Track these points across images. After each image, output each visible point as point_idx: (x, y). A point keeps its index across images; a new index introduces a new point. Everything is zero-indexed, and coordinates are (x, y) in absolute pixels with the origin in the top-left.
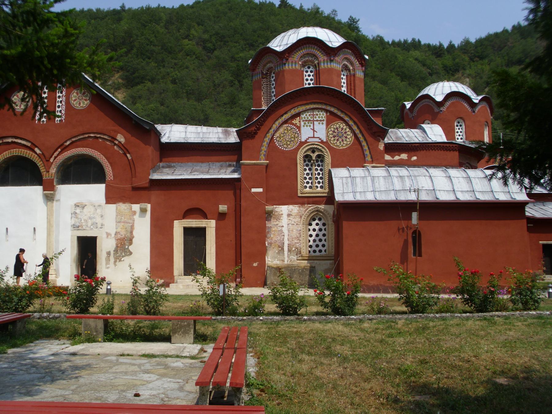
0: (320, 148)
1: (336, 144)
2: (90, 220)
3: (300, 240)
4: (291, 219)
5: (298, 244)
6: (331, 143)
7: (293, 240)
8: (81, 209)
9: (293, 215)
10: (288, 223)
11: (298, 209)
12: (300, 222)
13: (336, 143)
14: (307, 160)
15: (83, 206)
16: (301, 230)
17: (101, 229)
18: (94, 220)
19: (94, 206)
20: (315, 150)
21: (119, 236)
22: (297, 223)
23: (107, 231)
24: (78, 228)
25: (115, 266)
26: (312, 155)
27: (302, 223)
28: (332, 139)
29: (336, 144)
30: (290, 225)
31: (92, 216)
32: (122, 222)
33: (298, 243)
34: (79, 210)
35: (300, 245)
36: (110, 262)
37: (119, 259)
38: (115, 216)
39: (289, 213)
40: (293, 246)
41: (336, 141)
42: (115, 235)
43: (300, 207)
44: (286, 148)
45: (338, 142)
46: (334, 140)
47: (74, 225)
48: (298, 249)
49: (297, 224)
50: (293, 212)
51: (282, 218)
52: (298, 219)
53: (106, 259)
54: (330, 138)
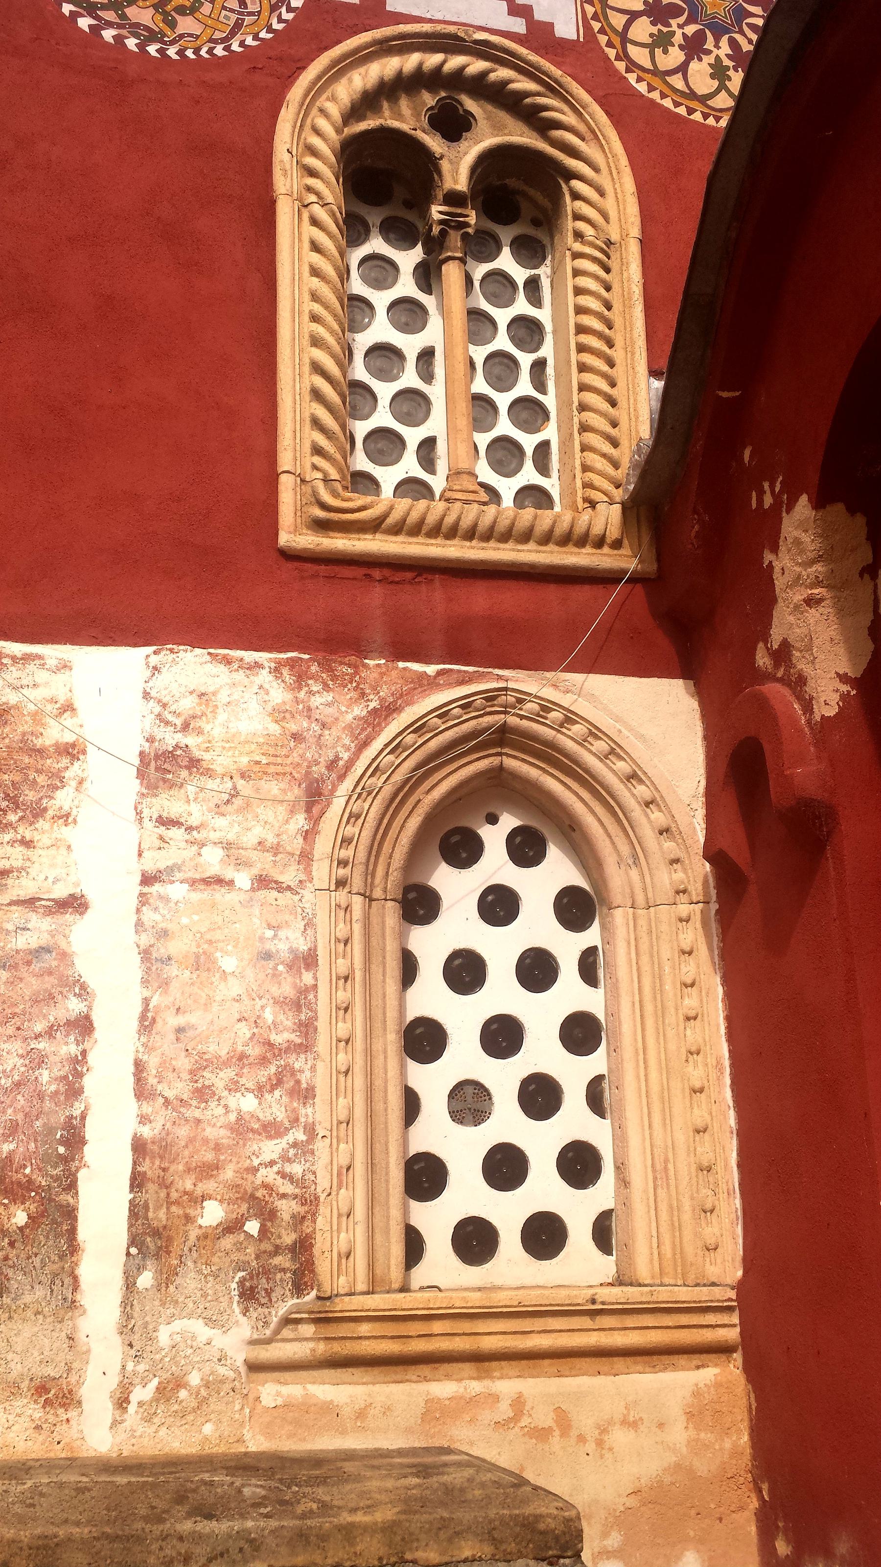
0: (524, 84)
1: (677, 82)
3: (307, 1095)
4: (196, 814)
5: (271, 1149)
6: (632, 66)
7: (203, 1094)
9: (221, 761)
10: (153, 861)
11: (278, 694)
12: (306, 858)
13: (683, 69)
14: (374, 217)
16: (309, 960)
20: (470, 104)
22: (263, 863)
26: (434, 143)
27: (322, 872)
28: (642, 29)
29: (677, 82)
30: (177, 891)
33: (272, 1130)
35: (303, 1149)
39: (170, 739)
40: (208, 1170)
41: (675, 56)
43: (301, 678)
44: (153, 36)
45: (700, 70)
46: (662, 41)
48: (268, 1215)
49: (263, 882)
50: (215, 728)
51: (63, 798)
52: (273, 814)
54: (618, 21)
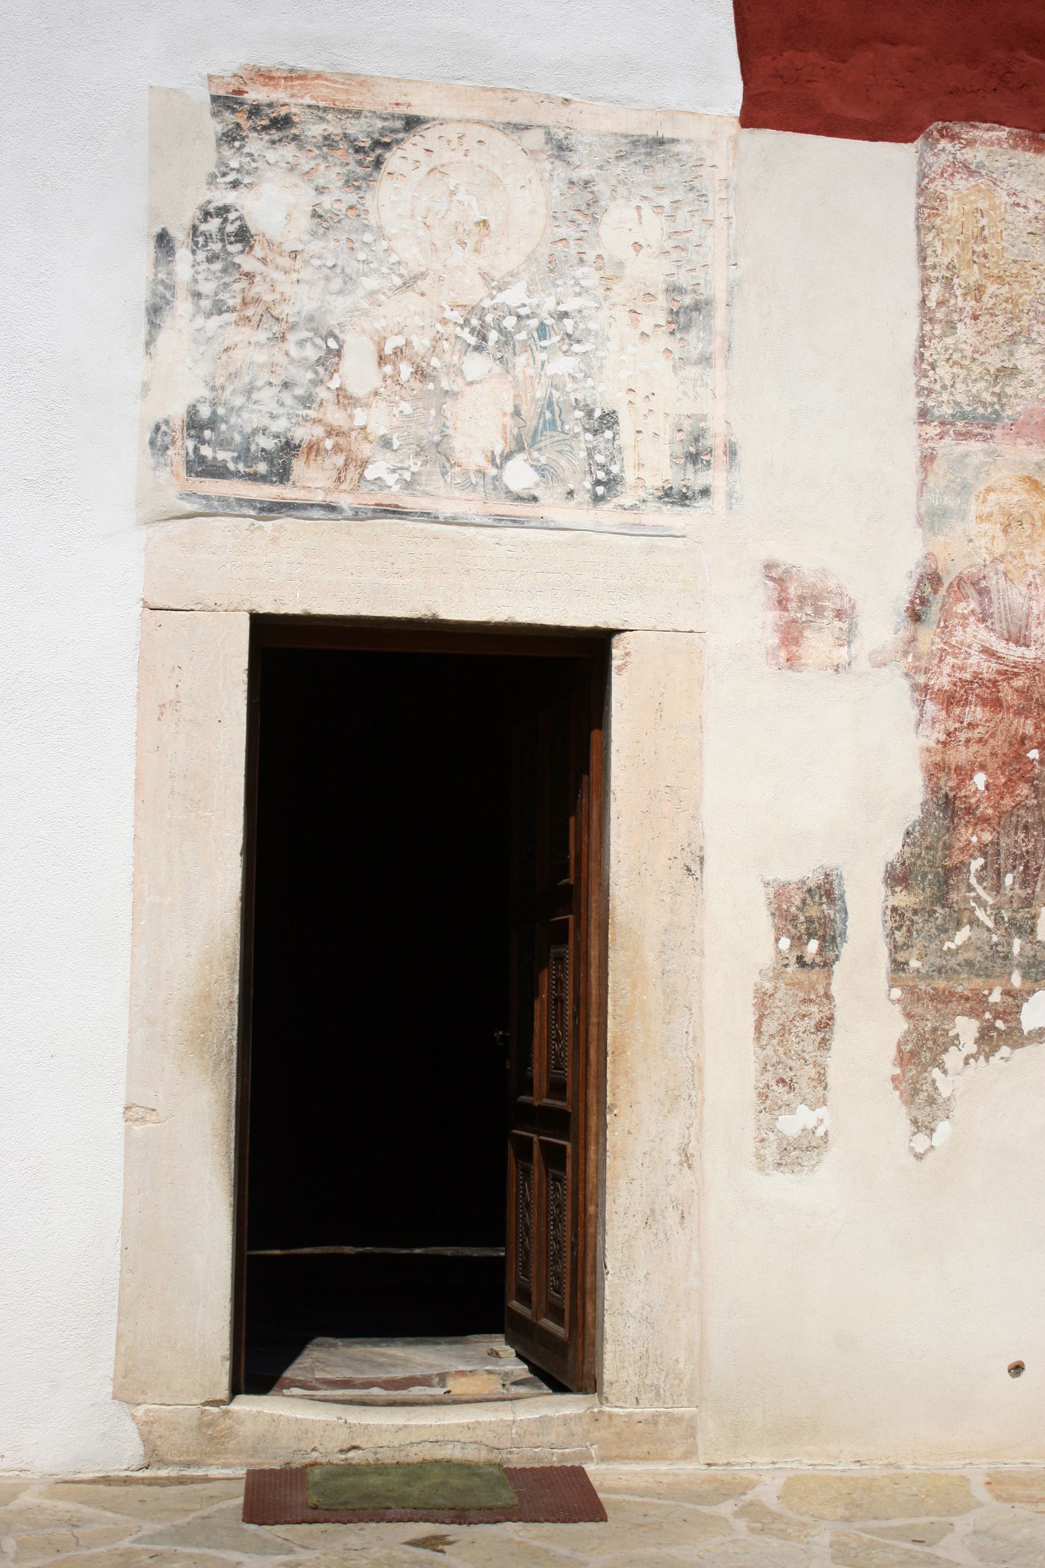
2: (476, 365)
8: (331, 175)
15: (356, 128)
17: (672, 517)
18: (562, 365)
19: (561, 149)
21: (976, 634)
23: (784, 555)
24: (283, 475)
25: (921, 1126)
31: (514, 296)
32: (1018, 429)
34: (305, 197)
36: (836, 1060)
37: (976, 1005)
38: (910, 328)
42: (916, 617)
47: (195, 425)
53: (763, 1002)
